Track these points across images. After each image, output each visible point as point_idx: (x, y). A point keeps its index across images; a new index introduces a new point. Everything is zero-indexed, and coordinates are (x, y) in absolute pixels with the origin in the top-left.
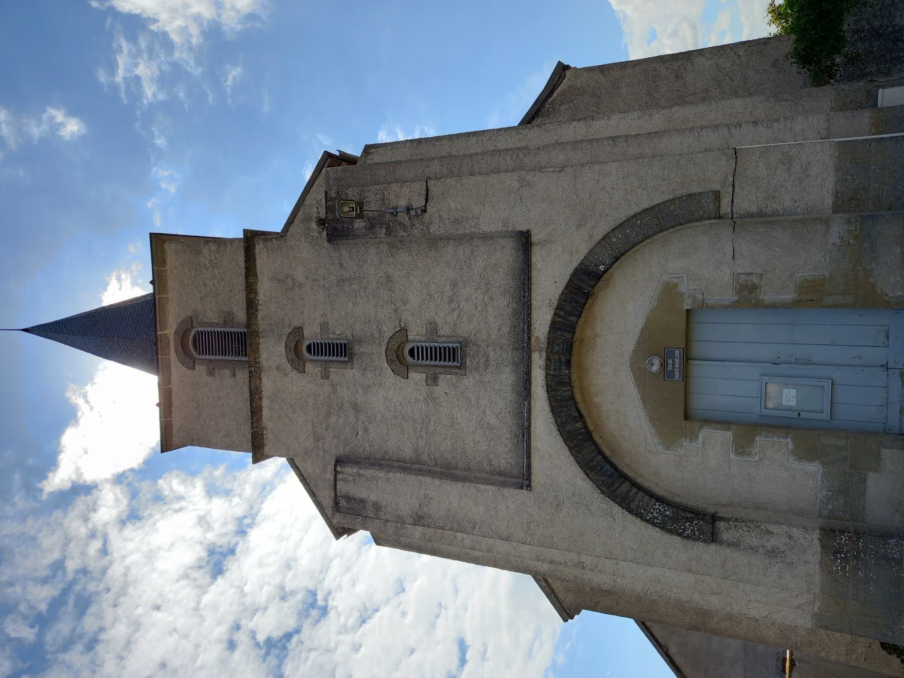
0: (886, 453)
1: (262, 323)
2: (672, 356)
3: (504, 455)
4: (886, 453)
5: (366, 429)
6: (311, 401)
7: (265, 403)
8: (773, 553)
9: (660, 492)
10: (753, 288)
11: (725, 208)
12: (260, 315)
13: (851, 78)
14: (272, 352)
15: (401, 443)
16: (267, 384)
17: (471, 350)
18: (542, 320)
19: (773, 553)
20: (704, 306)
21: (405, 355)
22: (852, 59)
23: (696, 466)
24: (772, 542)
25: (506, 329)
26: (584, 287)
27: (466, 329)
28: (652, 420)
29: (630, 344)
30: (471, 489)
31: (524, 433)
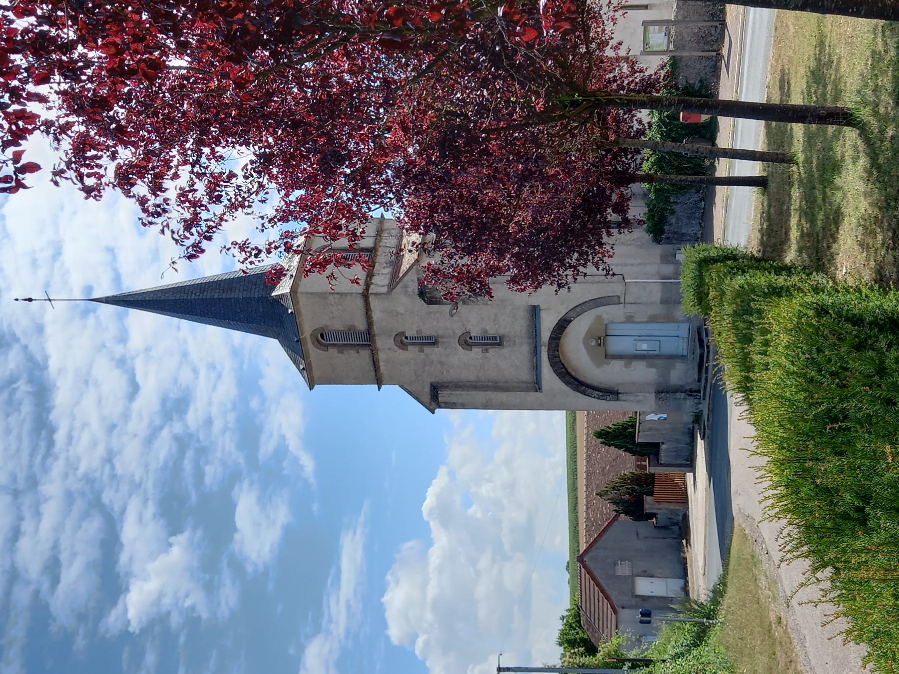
0: (677, 364)
1: (376, 329)
2: (599, 340)
3: (525, 375)
4: (677, 364)
5: (448, 371)
6: (412, 361)
7: (381, 364)
8: (639, 401)
9: (595, 384)
10: (632, 317)
11: (622, 300)
12: (375, 327)
13: (667, 243)
14: (384, 344)
15: (469, 375)
16: (382, 356)
17: (506, 339)
18: (545, 335)
19: (639, 401)
20: (612, 322)
21: (467, 342)
22: (668, 238)
23: (610, 373)
24: (638, 398)
25: (524, 331)
26: (562, 325)
27: (502, 331)
28: (591, 359)
29: (582, 335)
30: (513, 394)
31: (536, 368)
